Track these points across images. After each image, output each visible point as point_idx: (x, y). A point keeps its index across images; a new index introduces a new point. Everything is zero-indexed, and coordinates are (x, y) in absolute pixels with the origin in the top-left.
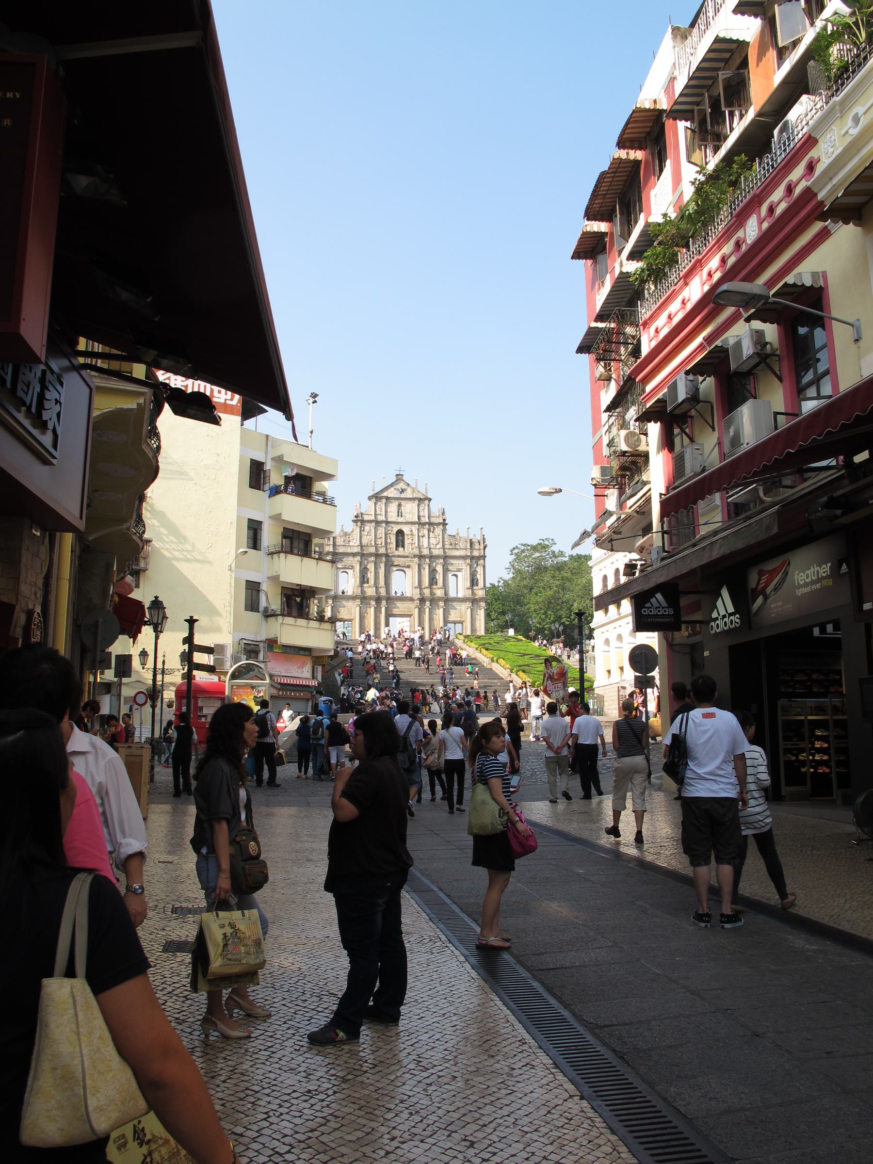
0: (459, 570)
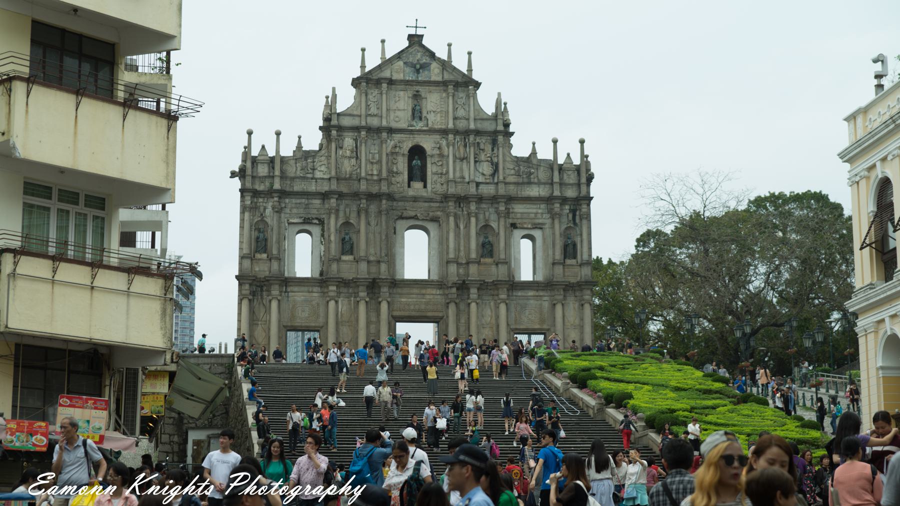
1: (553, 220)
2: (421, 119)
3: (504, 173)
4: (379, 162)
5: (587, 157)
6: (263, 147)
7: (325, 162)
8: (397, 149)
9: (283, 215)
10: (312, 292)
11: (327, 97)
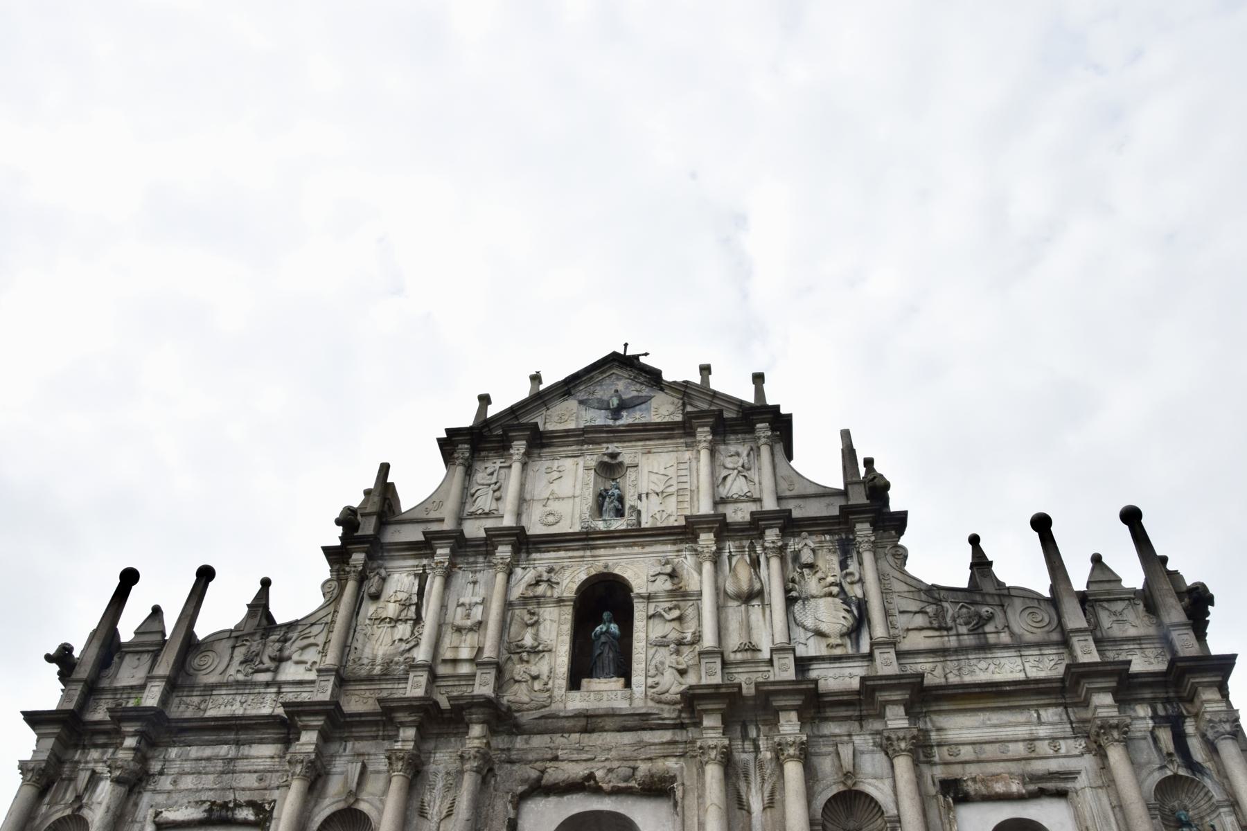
0: (1052, 787)
1: (1101, 754)
2: (620, 513)
3: (889, 625)
4: (480, 625)
5: (1164, 560)
6: (157, 611)
7: (320, 640)
8: (541, 589)
9: (146, 798)
11: (367, 493)
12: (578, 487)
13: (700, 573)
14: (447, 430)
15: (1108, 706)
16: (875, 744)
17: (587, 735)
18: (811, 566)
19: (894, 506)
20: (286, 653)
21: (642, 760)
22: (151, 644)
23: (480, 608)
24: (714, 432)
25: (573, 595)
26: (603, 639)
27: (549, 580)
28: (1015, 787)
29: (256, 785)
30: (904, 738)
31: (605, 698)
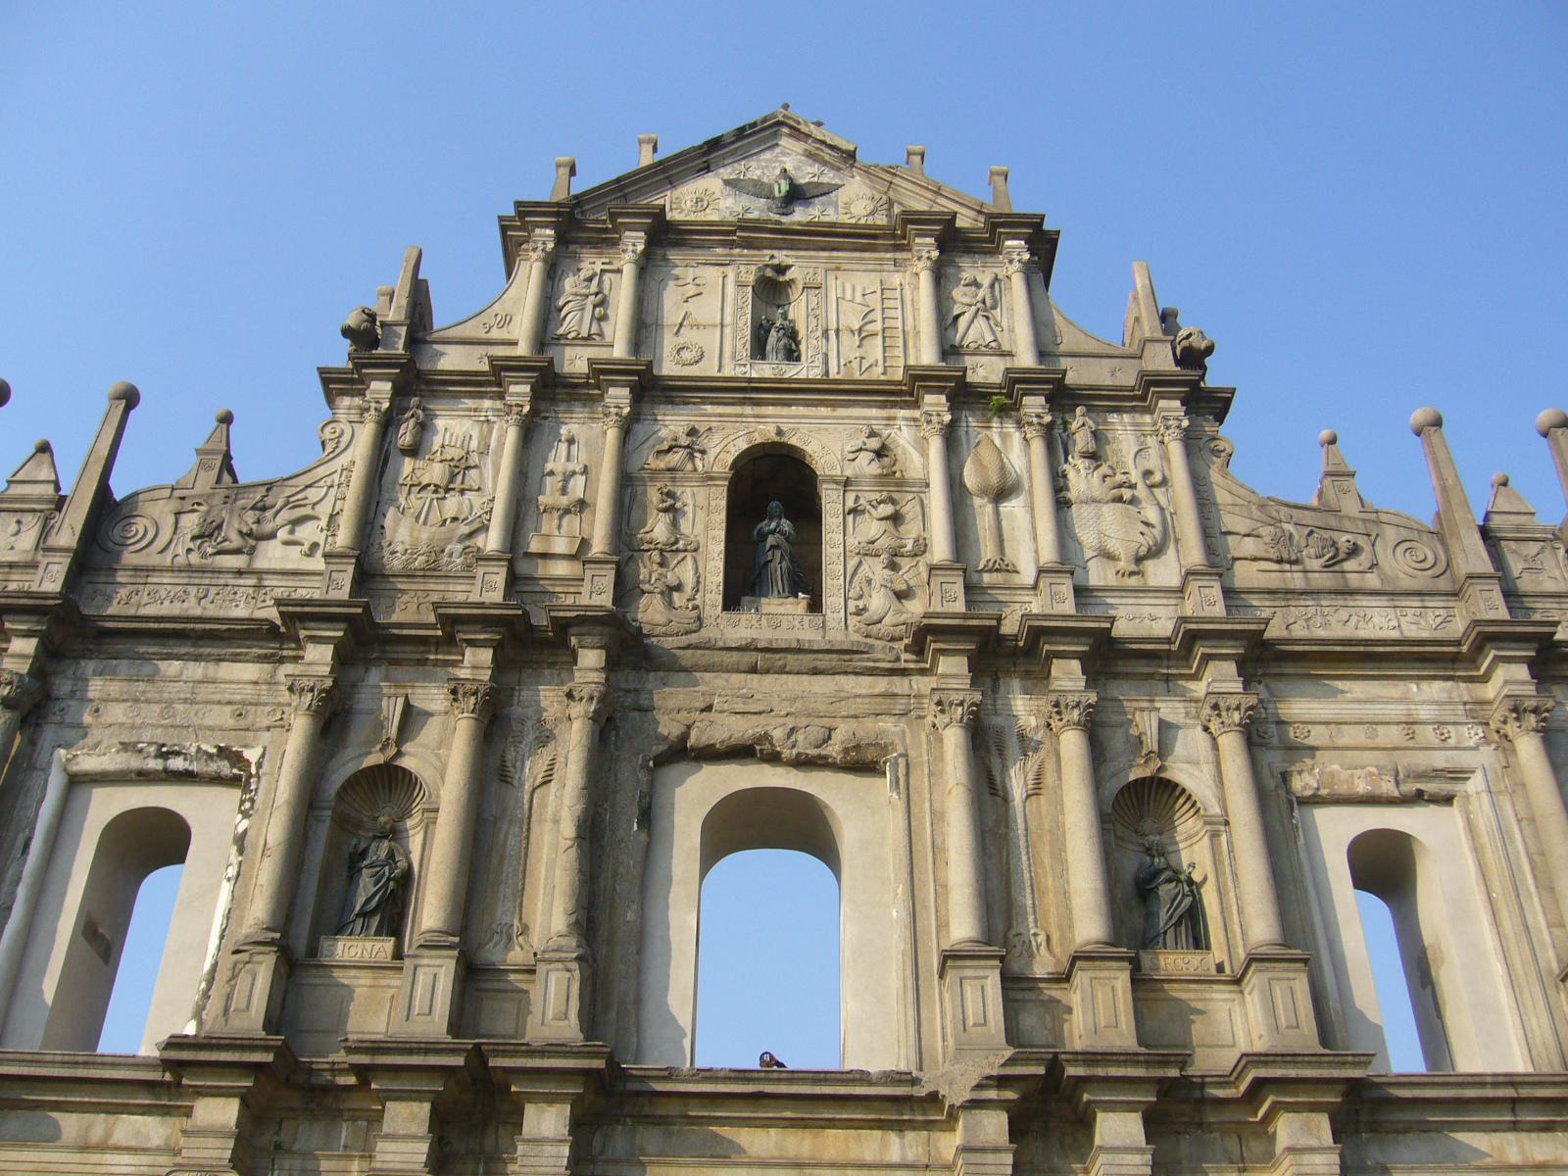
0: (1431, 791)
6: (44, 448)
7: (324, 510)
10: (104, 1147)
12: (728, 310)
13: (924, 454)
14: (518, 204)
15: (1523, 683)
16: (1187, 714)
17: (756, 677)
18: (1094, 457)
19: (1212, 380)
20: (268, 527)
21: (842, 717)
22: (39, 500)
23: (580, 480)
24: (941, 245)
25: (727, 470)
26: (771, 540)
27: (688, 447)
28: (1388, 788)
29: (231, 722)
30: (1238, 708)
31: (784, 625)
